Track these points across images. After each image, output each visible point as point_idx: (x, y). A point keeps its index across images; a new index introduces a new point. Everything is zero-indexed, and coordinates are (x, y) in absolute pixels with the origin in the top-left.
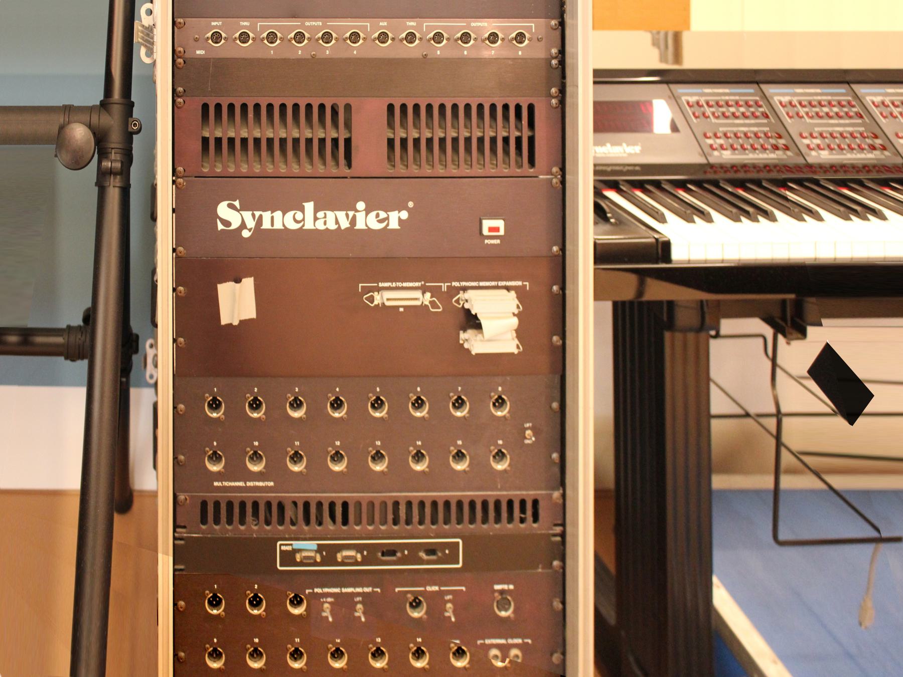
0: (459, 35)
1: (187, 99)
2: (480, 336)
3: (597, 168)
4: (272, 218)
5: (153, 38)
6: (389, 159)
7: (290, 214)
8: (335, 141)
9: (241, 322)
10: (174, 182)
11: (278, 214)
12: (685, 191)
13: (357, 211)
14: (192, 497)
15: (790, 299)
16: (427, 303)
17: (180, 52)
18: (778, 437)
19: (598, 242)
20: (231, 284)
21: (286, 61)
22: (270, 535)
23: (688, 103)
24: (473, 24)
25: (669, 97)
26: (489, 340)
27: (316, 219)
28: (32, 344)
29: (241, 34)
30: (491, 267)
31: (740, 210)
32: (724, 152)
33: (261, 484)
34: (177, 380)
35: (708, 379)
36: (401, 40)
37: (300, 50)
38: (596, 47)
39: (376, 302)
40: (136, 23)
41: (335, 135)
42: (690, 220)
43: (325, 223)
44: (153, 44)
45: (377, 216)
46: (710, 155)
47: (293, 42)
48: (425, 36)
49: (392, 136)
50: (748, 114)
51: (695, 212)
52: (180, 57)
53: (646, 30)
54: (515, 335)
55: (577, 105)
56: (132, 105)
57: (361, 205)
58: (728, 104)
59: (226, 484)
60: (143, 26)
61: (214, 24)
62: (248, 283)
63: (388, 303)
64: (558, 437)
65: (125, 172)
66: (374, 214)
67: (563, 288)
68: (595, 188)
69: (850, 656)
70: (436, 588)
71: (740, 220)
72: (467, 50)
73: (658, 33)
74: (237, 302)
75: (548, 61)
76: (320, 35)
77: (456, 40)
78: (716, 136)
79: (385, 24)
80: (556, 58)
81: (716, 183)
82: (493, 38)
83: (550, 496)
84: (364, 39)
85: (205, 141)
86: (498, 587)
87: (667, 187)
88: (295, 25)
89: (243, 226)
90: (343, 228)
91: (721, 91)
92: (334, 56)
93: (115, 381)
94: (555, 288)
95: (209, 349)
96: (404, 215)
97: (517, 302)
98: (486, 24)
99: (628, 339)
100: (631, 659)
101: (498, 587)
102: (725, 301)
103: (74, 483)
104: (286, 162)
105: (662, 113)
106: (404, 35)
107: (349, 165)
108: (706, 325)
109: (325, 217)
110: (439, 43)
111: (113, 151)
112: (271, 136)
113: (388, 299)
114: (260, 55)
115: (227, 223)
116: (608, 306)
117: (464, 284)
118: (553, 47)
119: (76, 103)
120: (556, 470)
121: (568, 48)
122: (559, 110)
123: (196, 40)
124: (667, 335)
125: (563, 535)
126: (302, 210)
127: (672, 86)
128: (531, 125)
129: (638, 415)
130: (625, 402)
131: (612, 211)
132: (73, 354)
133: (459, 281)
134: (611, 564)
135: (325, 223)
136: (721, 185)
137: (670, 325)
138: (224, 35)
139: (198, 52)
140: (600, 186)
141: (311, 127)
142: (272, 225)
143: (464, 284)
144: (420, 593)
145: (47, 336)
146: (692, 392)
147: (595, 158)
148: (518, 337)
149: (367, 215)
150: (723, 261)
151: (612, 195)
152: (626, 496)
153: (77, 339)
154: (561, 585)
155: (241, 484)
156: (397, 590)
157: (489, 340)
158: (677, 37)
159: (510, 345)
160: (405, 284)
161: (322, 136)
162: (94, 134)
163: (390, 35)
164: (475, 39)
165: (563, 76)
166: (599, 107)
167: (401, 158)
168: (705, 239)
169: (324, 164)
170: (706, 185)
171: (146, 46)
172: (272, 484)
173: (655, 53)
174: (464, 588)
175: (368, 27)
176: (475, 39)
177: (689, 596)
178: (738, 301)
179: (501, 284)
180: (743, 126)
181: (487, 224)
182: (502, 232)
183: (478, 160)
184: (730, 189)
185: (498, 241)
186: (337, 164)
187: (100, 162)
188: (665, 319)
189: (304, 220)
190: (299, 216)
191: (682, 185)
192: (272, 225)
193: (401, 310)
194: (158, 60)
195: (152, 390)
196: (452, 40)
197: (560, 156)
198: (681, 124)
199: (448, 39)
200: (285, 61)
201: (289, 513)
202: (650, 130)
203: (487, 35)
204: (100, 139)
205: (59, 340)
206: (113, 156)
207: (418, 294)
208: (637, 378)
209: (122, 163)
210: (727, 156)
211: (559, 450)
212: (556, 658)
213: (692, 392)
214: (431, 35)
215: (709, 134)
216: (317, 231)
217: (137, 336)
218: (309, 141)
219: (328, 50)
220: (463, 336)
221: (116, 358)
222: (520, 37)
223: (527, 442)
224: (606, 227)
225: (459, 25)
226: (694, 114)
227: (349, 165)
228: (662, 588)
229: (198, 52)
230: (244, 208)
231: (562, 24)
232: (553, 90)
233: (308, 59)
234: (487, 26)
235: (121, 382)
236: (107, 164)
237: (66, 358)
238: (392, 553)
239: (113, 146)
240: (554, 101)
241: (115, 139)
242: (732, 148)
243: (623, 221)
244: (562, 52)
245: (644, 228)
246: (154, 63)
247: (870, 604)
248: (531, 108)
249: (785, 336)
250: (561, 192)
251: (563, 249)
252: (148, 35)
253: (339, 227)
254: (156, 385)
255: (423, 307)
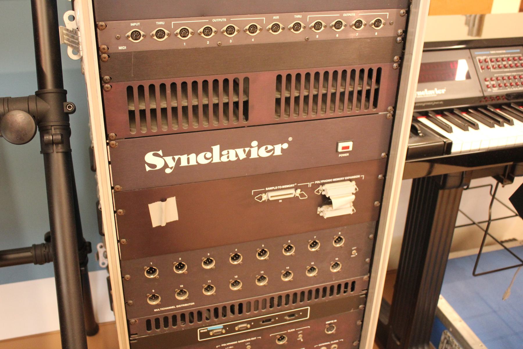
0: (334, 23)
1: (114, 84)
2: (330, 208)
3: (417, 105)
4: (188, 159)
5: (78, 39)
6: (276, 111)
7: (202, 155)
8: (236, 104)
9: (167, 224)
10: (108, 144)
11: (193, 156)
12: (466, 114)
13: (252, 147)
14: (139, 320)
15: (510, 165)
16: (298, 195)
17: (104, 49)
18: (486, 232)
19: (410, 147)
20: (159, 203)
21: (196, 50)
22: (193, 327)
23: (479, 61)
24: (345, 15)
25: (469, 58)
26: (336, 210)
27: (221, 155)
28: (6, 260)
29: (157, 32)
30: (339, 170)
31: (495, 120)
32: (494, 89)
33: (186, 305)
34: (122, 262)
35: (458, 210)
36: (290, 29)
37: (208, 41)
38: (429, 26)
39: (263, 199)
40: (61, 28)
41: (236, 100)
42: (465, 129)
43: (228, 157)
44: (78, 44)
45: (266, 148)
46: (486, 91)
47: (203, 35)
48: (308, 25)
49: (279, 96)
50: (513, 65)
51: (470, 125)
52: (105, 53)
53: (463, 15)
54: (352, 204)
55: (410, 67)
56: (65, 92)
57: (255, 143)
58: (503, 60)
59: (163, 309)
60: (68, 30)
61: (132, 24)
62: (172, 201)
63: (271, 199)
64: (370, 251)
65: (65, 140)
66: (264, 147)
67: (385, 176)
68: (413, 116)
69: (495, 312)
70: (294, 330)
71: (494, 127)
72: (338, 34)
73: (470, 16)
74: (163, 213)
75: (395, 38)
76: (225, 28)
77: (331, 27)
78: (491, 80)
79: (278, 17)
80: (400, 36)
81: (485, 107)
82: (358, 24)
83: (362, 278)
84: (261, 30)
85: (132, 113)
86: (327, 323)
87: (456, 112)
88: (204, 22)
89: (166, 166)
90: (241, 158)
91: (501, 52)
92: (236, 44)
93: (76, 270)
94: (380, 176)
95: (141, 241)
96: (285, 146)
97: (356, 187)
98: (354, 15)
99: (418, 197)
100: (393, 335)
101: (327, 323)
102: (475, 170)
103: (55, 326)
104: (198, 121)
105: (463, 67)
106: (292, 25)
107: (247, 119)
108: (463, 183)
109: (228, 153)
110: (318, 29)
111: (53, 128)
112: (186, 104)
113: (271, 197)
114: (174, 46)
115: (153, 166)
116: (410, 182)
117: (323, 181)
118: (399, 29)
119: (13, 96)
120: (368, 266)
121: (410, 29)
122: (398, 70)
123: (118, 38)
124: (440, 192)
125: (366, 294)
126: (211, 151)
127: (472, 51)
128: (378, 81)
129: (417, 233)
130: (411, 228)
131: (422, 129)
132: (40, 260)
133: (320, 180)
134: (390, 301)
135: (228, 157)
136: (488, 108)
137: (443, 187)
138: (142, 33)
139: (120, 48)
140: (416, 115)
141: (197, 96)
142: (188, 162)
143: (323, 181)
144: (284, 334)
145: (18, 253)
146: (448, 218)
147: (416, 99)
148: (354, 205)
149: (258, 149)
150: (479, 150)
151: (423, 120)
152: (403, 271)
153: (44, 251)
154: (362, 315)
155: (173, 307)
156: (271, 335)
157: (336, 210)
158: (482, 19)
159: (349, 210)
160: (283, 187)
161: (226, 101)
162: (34, 117)
163: (281, 26)
164: (345, 26)
165: (404, 48)
166: (423, 66)
167: (285, 111)
168: (467, 140)
169: (228, 120)
170: (479, 109)
171: (72, 46)
172: (193, 303)
173: (466, 29)
174: (309, 327)
175: (263, 21)
176: (345, 26)
177: (426, 305)
178: (483, 169)
179: (346, 178)
180: (508, 72)
181: (341, 145)
182: (351, 149)
183: (339, 107)
184: (492, 110)
185: (348, 154)
186: (238, 119)
187: (42, 137)
188: (441, 183)
189: (212, 157)
190: (209, 155)
191: (465, 110)
192: (188, 162)
193: (280, 201)
194: (84, 55)
195: (106, 271)
196: (328, 27)
197: (394, 99)
198: (473, 74)
199: (325, 27)
200: (196, 50)
201: (205, 315)
202: (453, 79)
203: (354, 22)
204: (41, 122)
205: (29, 254)
206: (53, 131)
207: (292, 191)
208: (420, 216)
209: (62, 135)
210: (496, 91)
211: (370, 256)
212: (355, 344)
213: (448, 218)
214: (313, 24)
215: (488, 79)
216: (222, 163)
217: (90, 243)
218: (216, 106)
219: (231, 39)
220: (319, 209)
221: (75, 257)
222: (378, 23)
223: (352, 256)
224: (417, 139)
225: (334, 16)
226: (481, 67)
227: (247, 119)
228: (414, 305)
229: (120, 48)
230: (165, 154)
231: (408, 12)
232: (396, 58)
233: (215, 47)
234: (355, 15)
235: (81, 271)
236: (48, 137)
237: (36, 263)
238: (270, 320)
239: (52, 124)
240: (395, 65)
241: (53, 118)
242: (499, 86)
243: (428, 133)
244: (405, 32)
245: (438, 136)
246: (81, 59)
247: (509, 291)
248: (379, 71)
249: (502, 183)
250: (391, 121)
251: (388, 155)
252: (73, 37)
253: (239, 158)
254: (107, 268)
255: (295, 198)
